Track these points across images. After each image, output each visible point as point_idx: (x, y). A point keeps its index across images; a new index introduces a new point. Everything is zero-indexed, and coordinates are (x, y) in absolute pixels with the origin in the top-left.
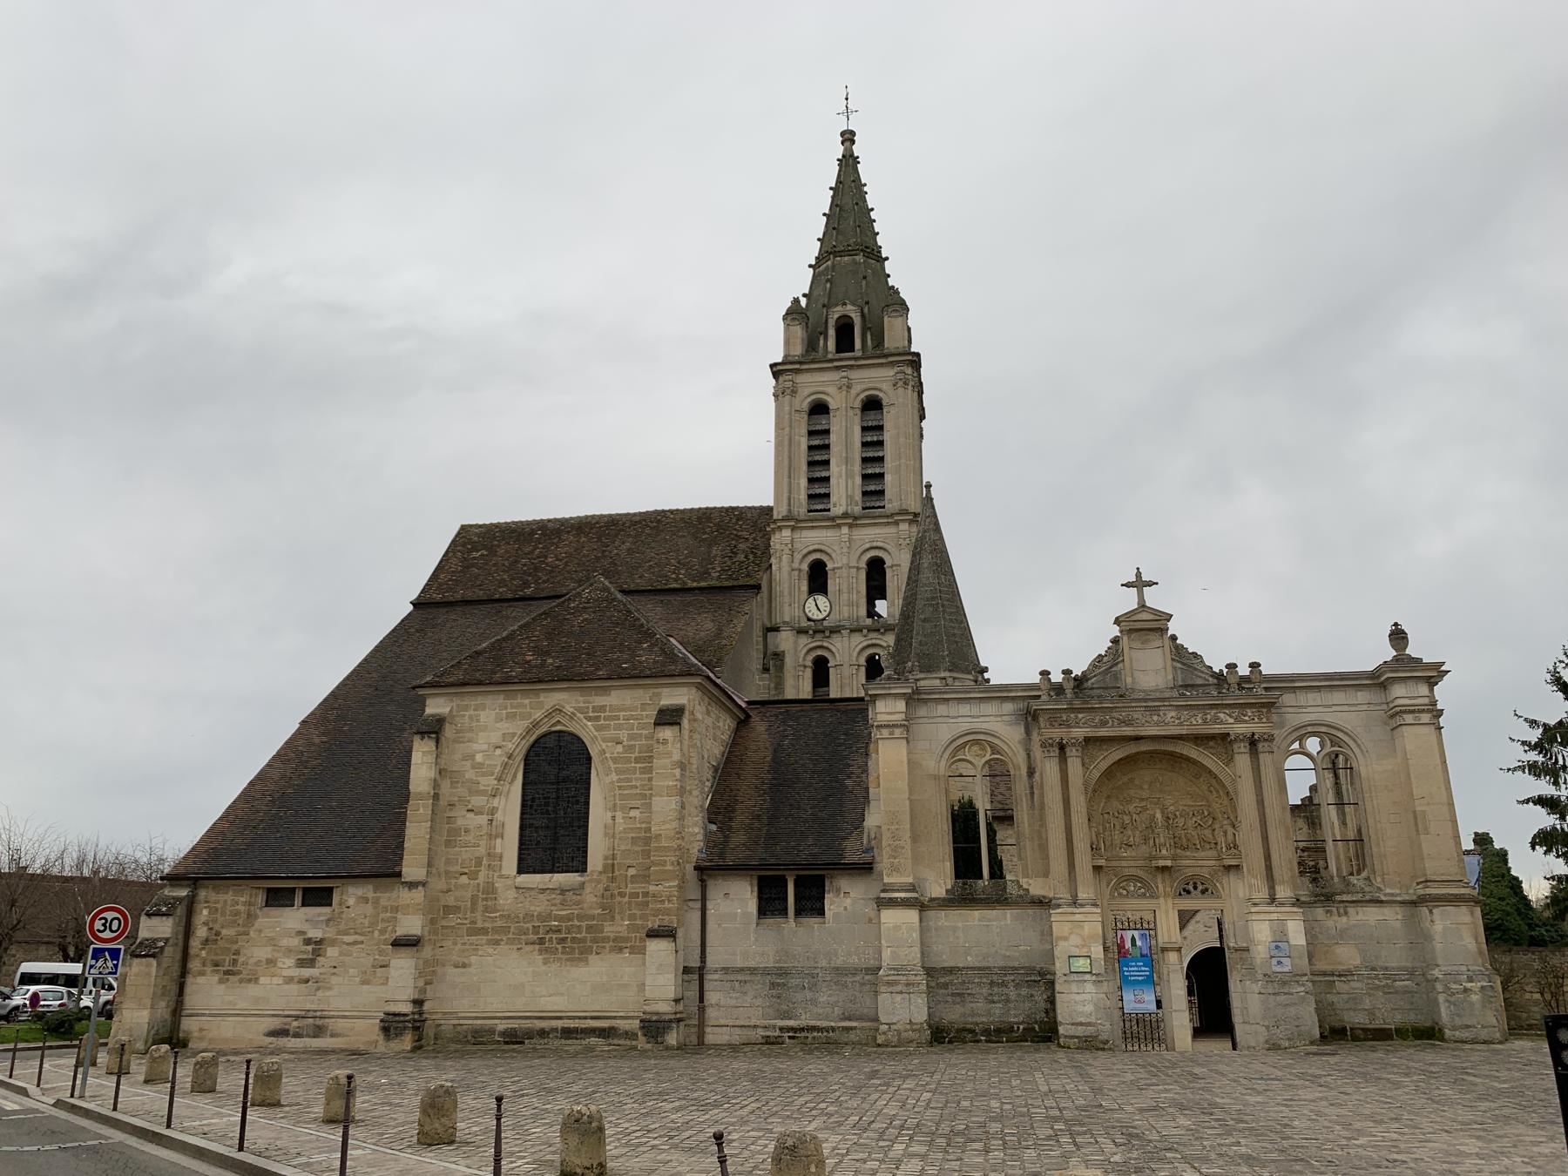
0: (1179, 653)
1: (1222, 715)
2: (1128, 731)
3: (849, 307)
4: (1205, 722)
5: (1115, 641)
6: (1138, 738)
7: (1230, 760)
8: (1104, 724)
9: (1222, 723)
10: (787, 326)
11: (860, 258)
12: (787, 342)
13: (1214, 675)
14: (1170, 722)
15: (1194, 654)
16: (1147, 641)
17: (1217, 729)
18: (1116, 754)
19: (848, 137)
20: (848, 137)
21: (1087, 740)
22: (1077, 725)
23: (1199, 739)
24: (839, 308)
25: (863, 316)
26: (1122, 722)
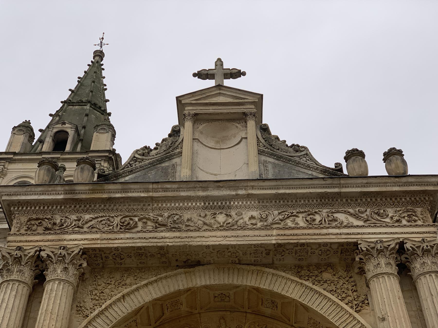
0: (269, 144)
1: (341, 217)
2: (168, 238)
3: (67, 125)
4: (311, 223)
5: (175, 132)
6: (190, 260)
7: (362, 303)
8: (127, 227)
9: (341, 225)
10: (13, 134)
11: (88, 107)
12: (10, 144)
13: (325, 170)
14: (249, 227)
15: (296, 148)
16: (224, 139)
17: (334, 235)
18: (148, 292)
19: (99, 55)
20: (99, 55)
21: (96, 265)
22: (79, 228)
23: (309, 261)
24: (60, 126)
25: (77, 131)
26: (159, 225)
